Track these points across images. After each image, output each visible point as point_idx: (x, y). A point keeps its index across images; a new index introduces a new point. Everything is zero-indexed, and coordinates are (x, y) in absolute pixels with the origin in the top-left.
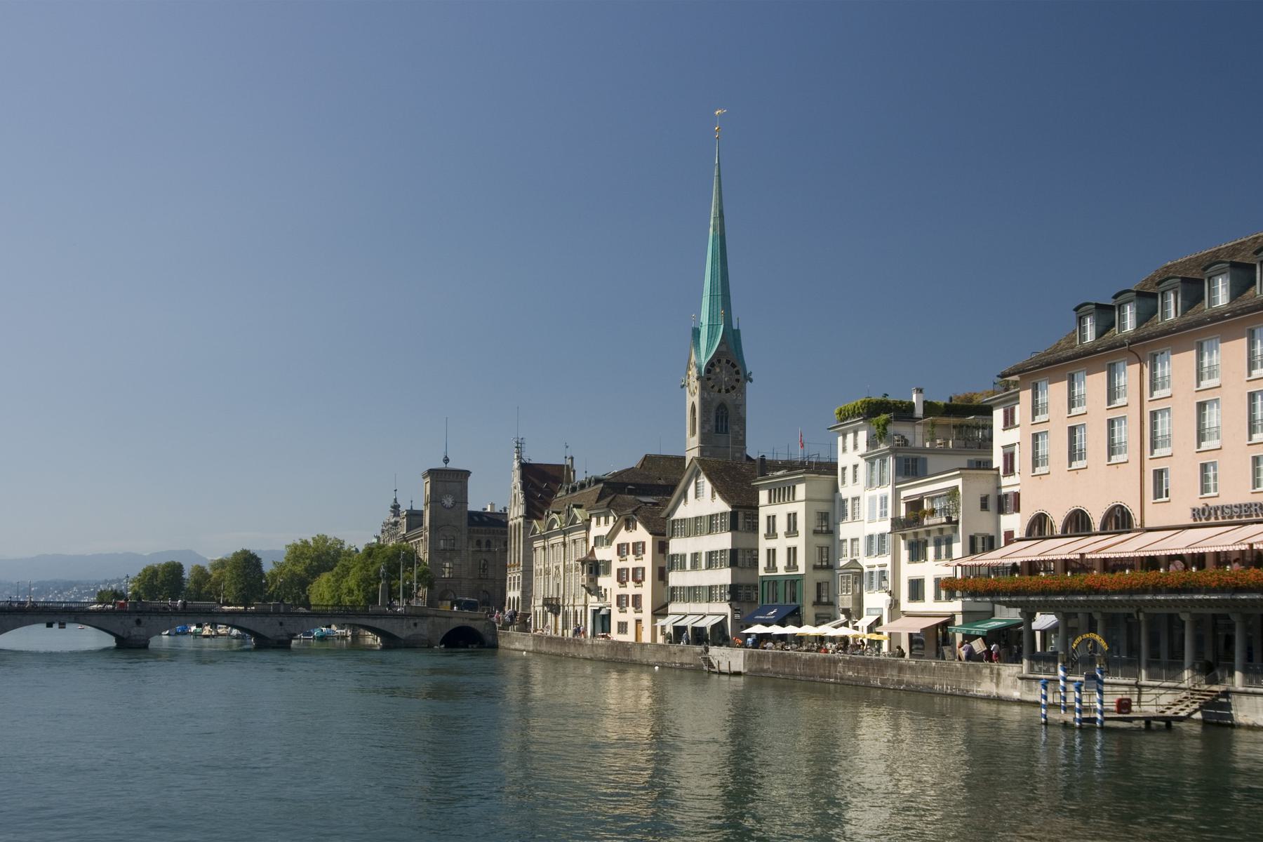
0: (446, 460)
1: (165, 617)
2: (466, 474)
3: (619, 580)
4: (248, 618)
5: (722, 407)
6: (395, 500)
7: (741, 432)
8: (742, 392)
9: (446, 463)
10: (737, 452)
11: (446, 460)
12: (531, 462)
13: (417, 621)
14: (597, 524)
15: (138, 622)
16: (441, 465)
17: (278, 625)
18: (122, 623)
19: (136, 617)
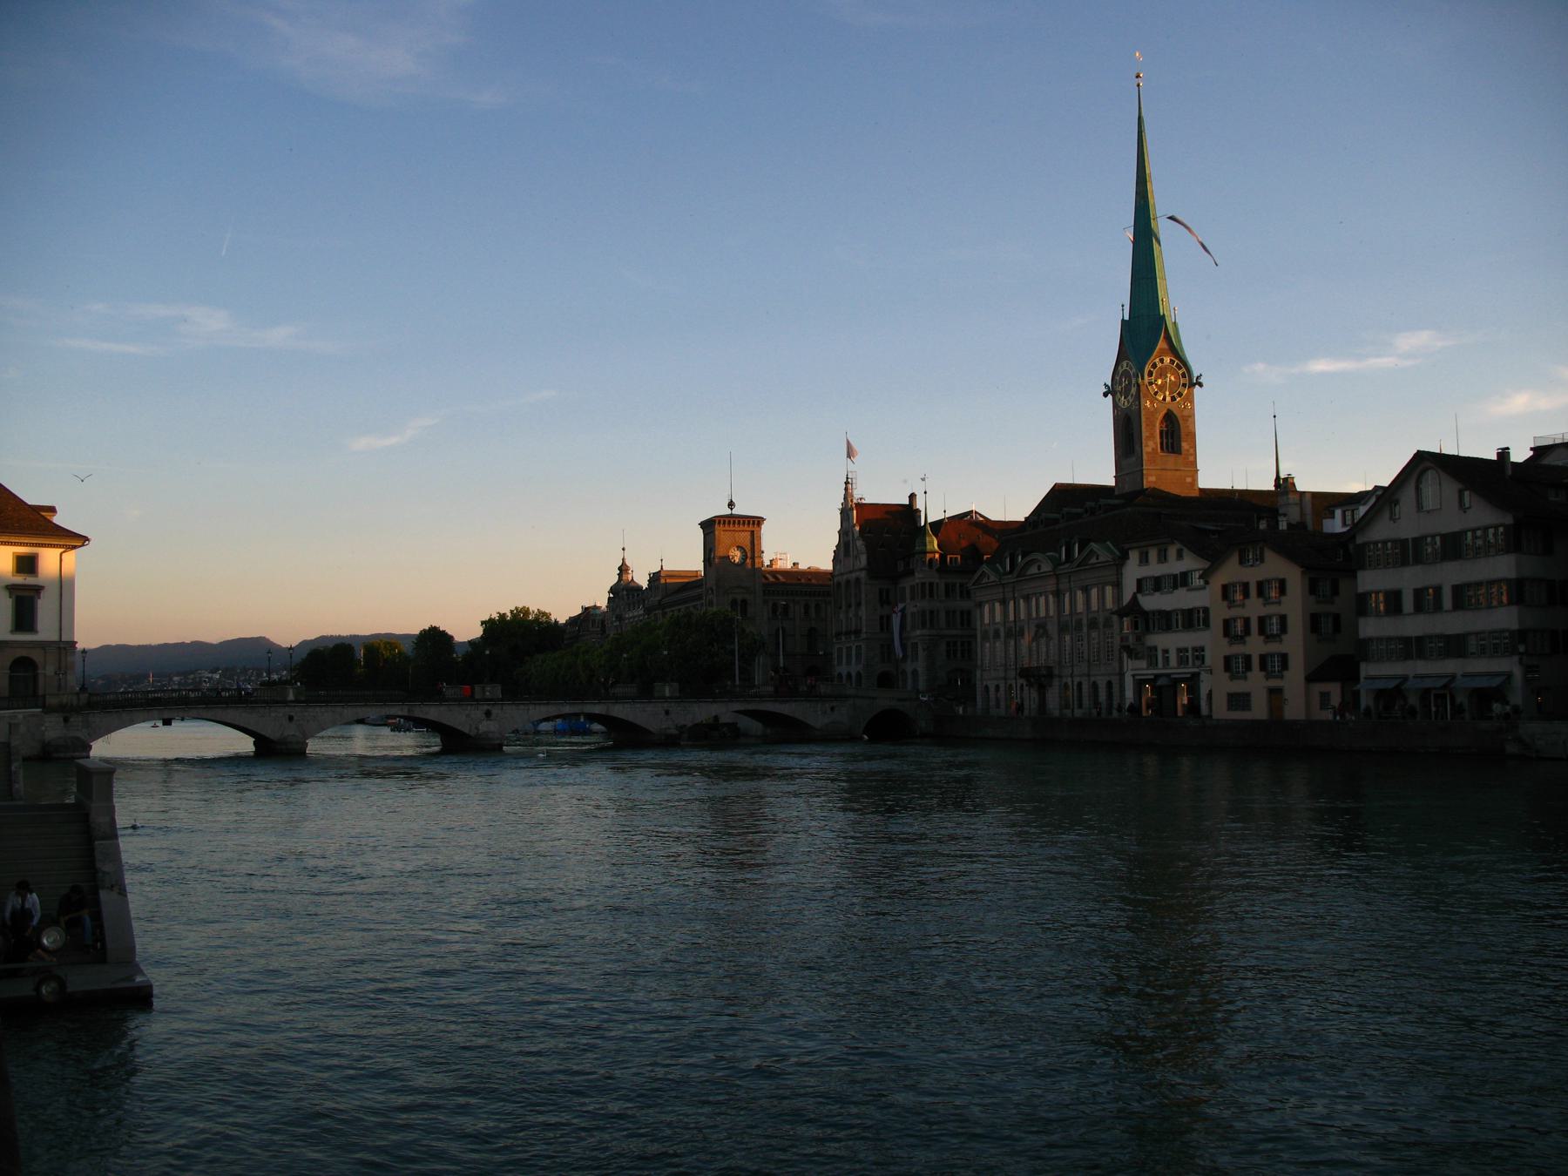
0: (731, 505)
1: (522, 707)
2: (757, 521)
3: (1226, 633)
4: (626, 705)
5: (1170, 418)
6: (623, 559)
7: (1191, 451)
8: (1190, 398)
9: (732, 509)
10: (1189, 476)
11: (731, 505)
12: (863, 501)
13: (834, 704)
14: (1141, 562)
15: (488, 714)
16: (728, 512)
17: (663, 712)
18: (468, 716)
19: (486, 707)
